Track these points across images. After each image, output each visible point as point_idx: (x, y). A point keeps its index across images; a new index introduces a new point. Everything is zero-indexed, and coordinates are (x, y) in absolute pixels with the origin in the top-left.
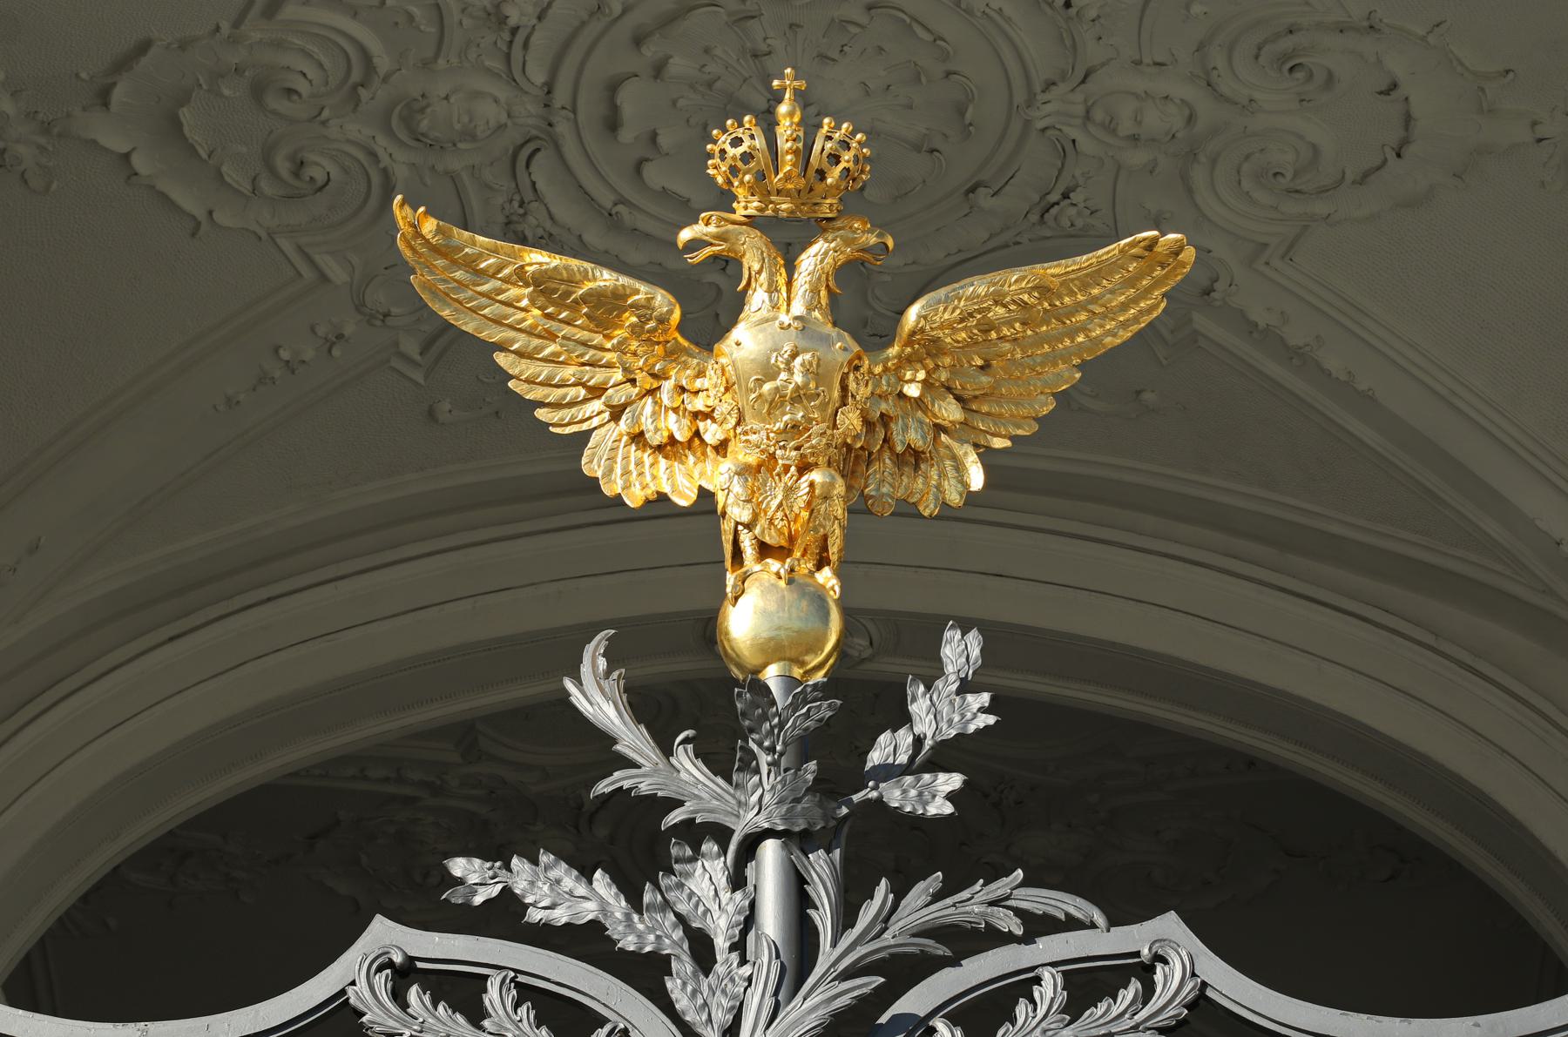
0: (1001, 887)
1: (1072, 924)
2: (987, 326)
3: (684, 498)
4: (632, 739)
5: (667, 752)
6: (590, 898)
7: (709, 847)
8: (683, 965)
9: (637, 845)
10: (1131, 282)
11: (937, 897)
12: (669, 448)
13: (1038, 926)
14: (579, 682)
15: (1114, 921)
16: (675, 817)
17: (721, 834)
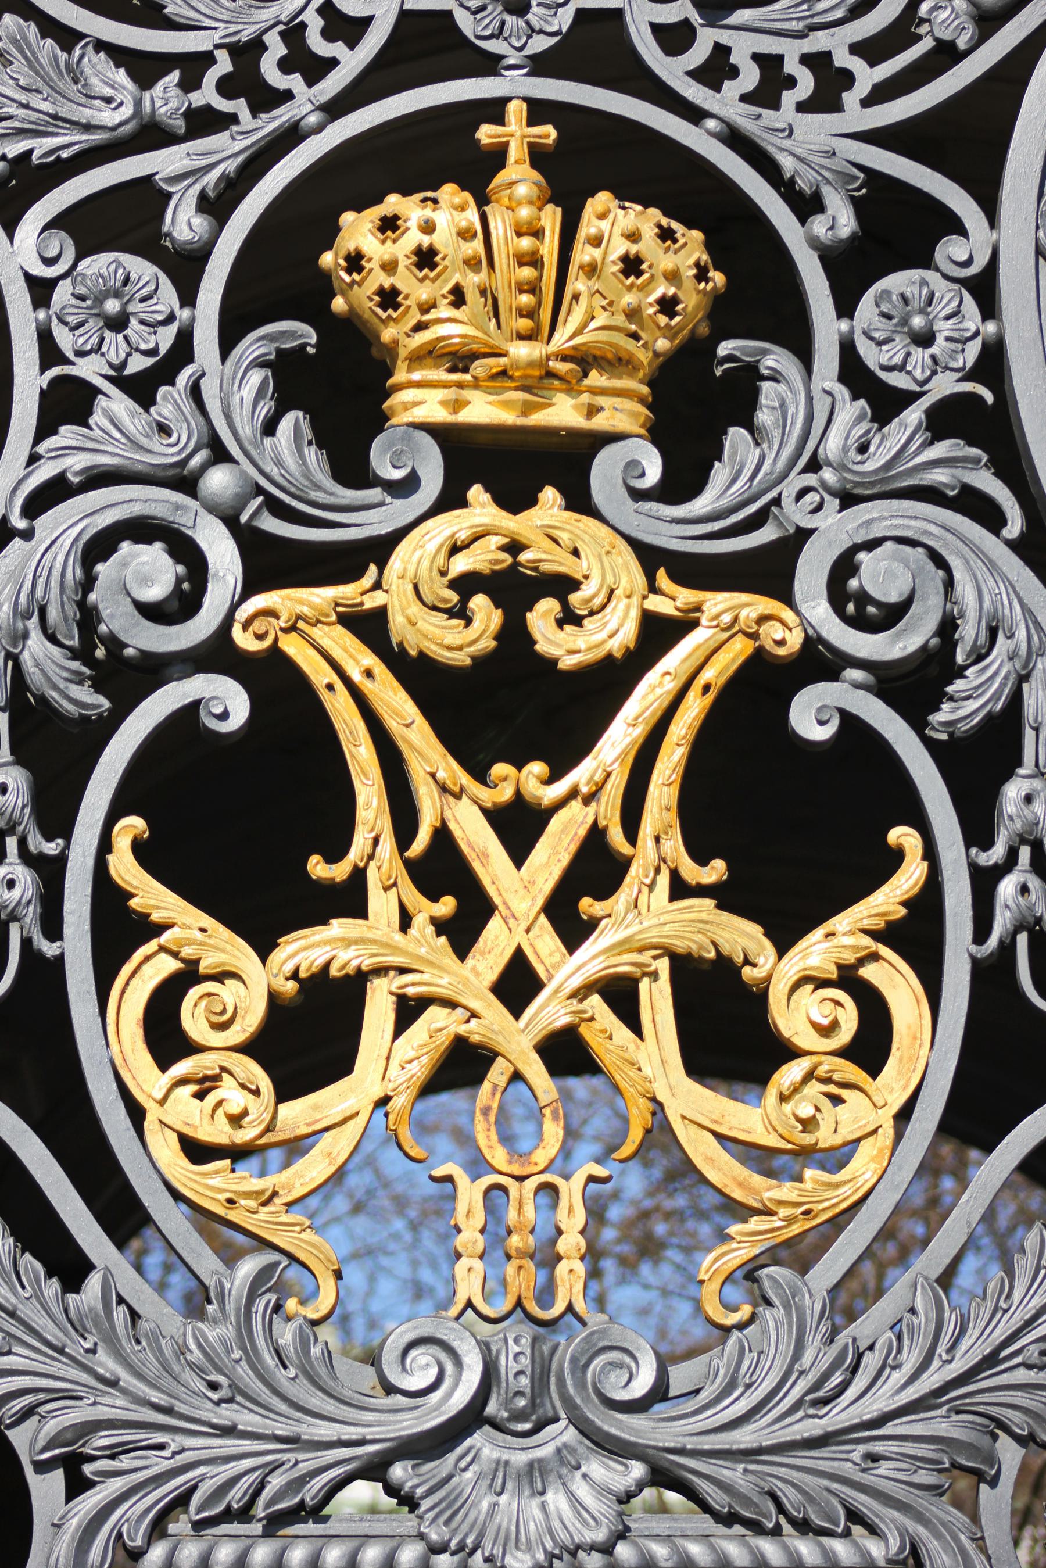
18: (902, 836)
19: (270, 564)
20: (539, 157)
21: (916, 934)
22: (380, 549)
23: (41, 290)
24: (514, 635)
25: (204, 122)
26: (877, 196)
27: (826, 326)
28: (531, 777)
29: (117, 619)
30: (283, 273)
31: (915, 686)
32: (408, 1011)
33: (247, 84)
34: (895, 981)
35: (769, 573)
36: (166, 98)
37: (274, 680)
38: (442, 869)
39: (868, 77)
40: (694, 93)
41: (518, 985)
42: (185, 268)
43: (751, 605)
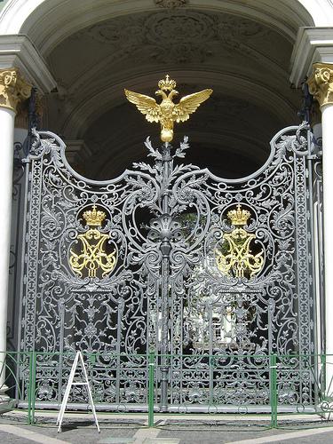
0: (190, 165)
4: (152, 150)
9: (152, 161)
13: (193, 170)
19: (79, 233)
21: (115, 255)
30: (81, 215)
31: (115, 240)
34: (114, 258)
35: (108, 233)
37: (79, 240)
38: (89, 251)
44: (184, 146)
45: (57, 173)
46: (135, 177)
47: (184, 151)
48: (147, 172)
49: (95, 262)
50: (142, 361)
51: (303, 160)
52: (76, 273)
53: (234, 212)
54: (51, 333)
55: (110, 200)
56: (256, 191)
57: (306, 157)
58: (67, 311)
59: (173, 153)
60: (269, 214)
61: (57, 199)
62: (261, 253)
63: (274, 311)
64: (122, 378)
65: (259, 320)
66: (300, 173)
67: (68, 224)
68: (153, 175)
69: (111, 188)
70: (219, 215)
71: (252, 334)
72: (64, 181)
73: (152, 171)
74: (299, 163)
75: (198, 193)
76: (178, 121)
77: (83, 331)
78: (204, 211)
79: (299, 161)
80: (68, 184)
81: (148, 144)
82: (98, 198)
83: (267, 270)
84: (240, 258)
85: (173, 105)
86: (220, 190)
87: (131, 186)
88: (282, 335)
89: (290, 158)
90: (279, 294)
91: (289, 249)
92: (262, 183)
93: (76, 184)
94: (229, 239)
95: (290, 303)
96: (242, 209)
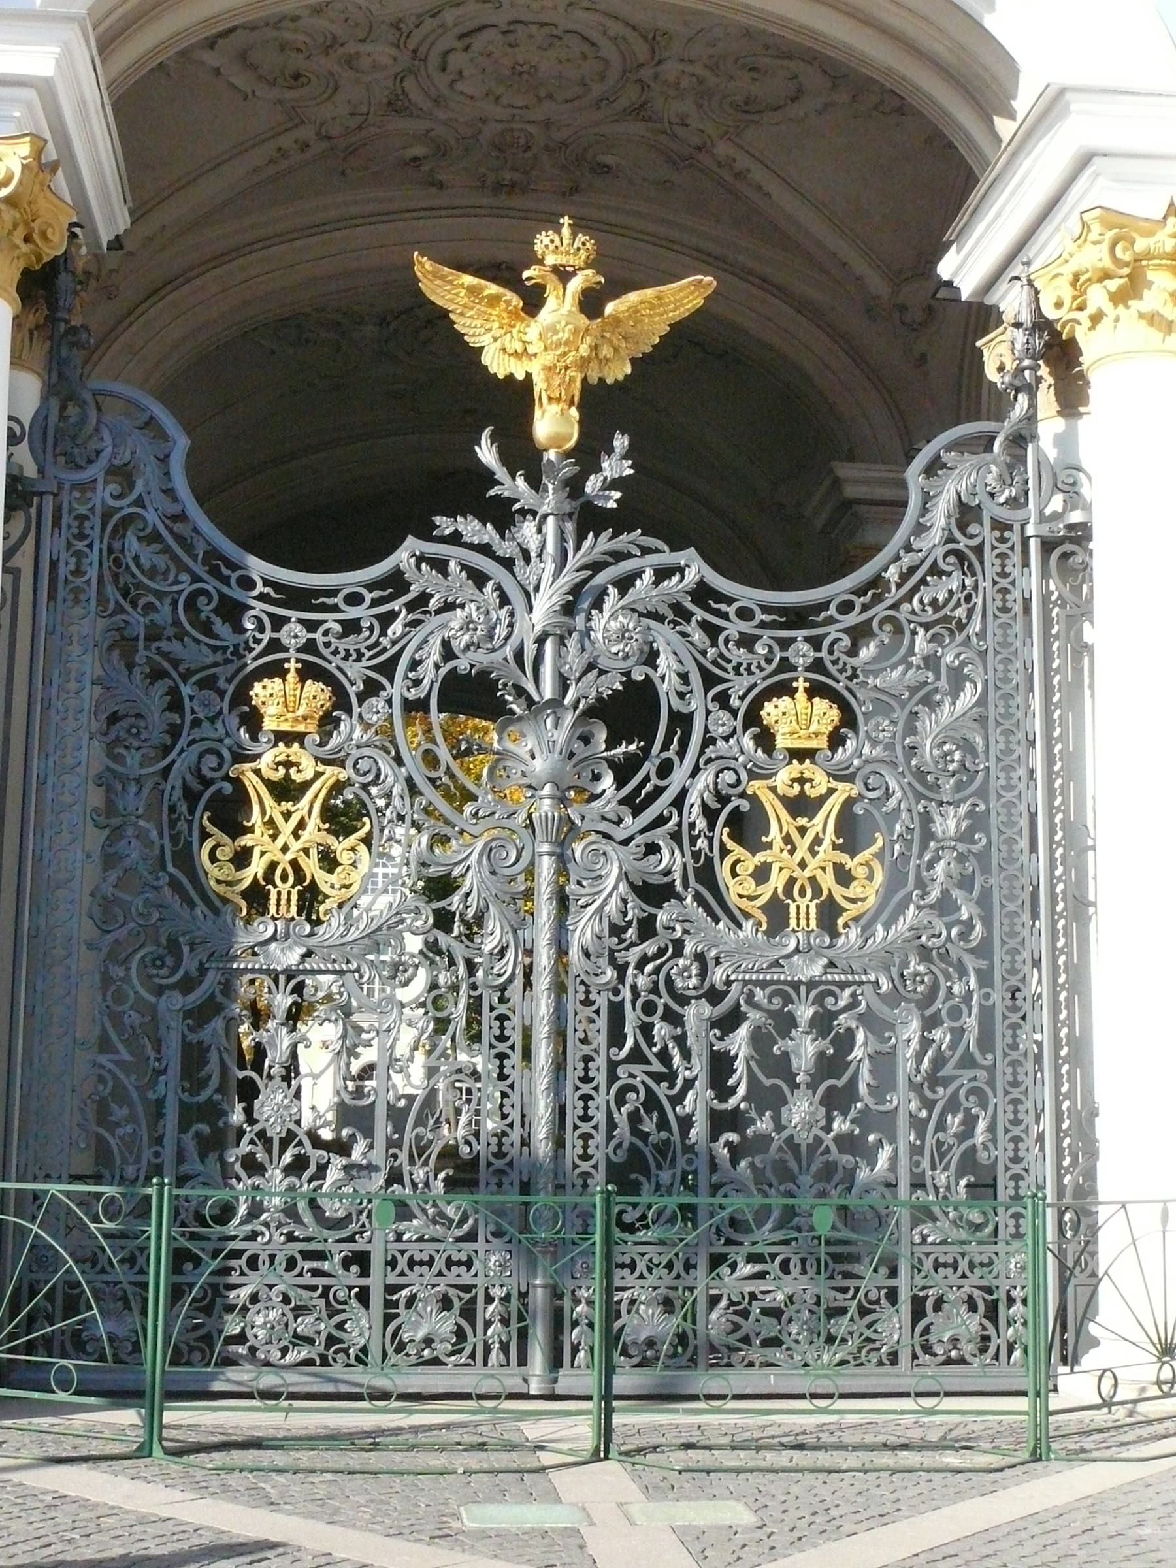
1: (657, 551)
2: (637, 311)
3: (520, 376)
4: (501, 473)
5: (514, 478)
6: (489, 534)
7: (529, 517)
8: (520, 563)
9: (503, 515)
10: (692, 293)
11: (611, 539)
12: (516, 354)
13: (646, 551)
14: (479, 445)
15: (672, 550)
16: (517, 506)
17: (534, 513)
18: (366, 819)
20: (297, 670)
22: (259, 756)
23: (191, 698)
24: (287, 774)
25: (227, 661)
26: (368, 681)
27: (356, 710)
28: (289, 806)
29: (205, 771)
32: (263, 853)
33: (236, 652)
36: (219, 657)
38: (271, 823)
39: (368, 654)
40: (331, 657)
41: (285, 849)
42: (222, 694)
43: (336, 770)
44: (616, 466)
45: (155, 537)
46: (440, 565)
47: (615, 484)
48: (485, 549)
49: (294, 863)
50: (464, 1219)
51: (1015, 537)
52: (225, 901)
53: (785, 702)
54: (132, 1118)
55: (350, 643)
56: (859, 634)
57: (1023, 527)
58: (193, 1037)
59: (574, 486)
60: (901, 715)
61: (154, 634)
62: (874, 849)
63: (915, 1044)
64: (392, 1279)
65: (865, 1075)
66: (1004, 583)
67: (196, 723)
68: (508, 563)
69: (354, 599)
70: (734, 713)
71: (840, 1125)
72: (182, 567)
73: (505, 548)
74: (1003, 548)
75: (663, 636)
76: (594, 379)
77: (249, 1111)
78: (681, 695)
79: (1003, 540)
80: (196, 579)
81: (487, 453)
82: (304, 635)
83: (890, 907)
84: (803, 865)
85: (583, 320)
86: (735, 628)
87: (424, 598)
88: (941, 1126)
89: (973, 529)
90: (934, 988)
91: (966, 837)
92: (880, 611)
93: (226, 581)
94: (767, 798)
95: (971, 1022)
96: (811, 693)
